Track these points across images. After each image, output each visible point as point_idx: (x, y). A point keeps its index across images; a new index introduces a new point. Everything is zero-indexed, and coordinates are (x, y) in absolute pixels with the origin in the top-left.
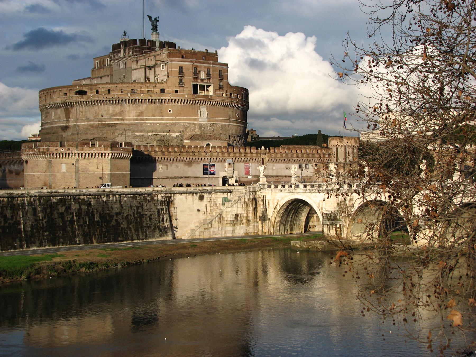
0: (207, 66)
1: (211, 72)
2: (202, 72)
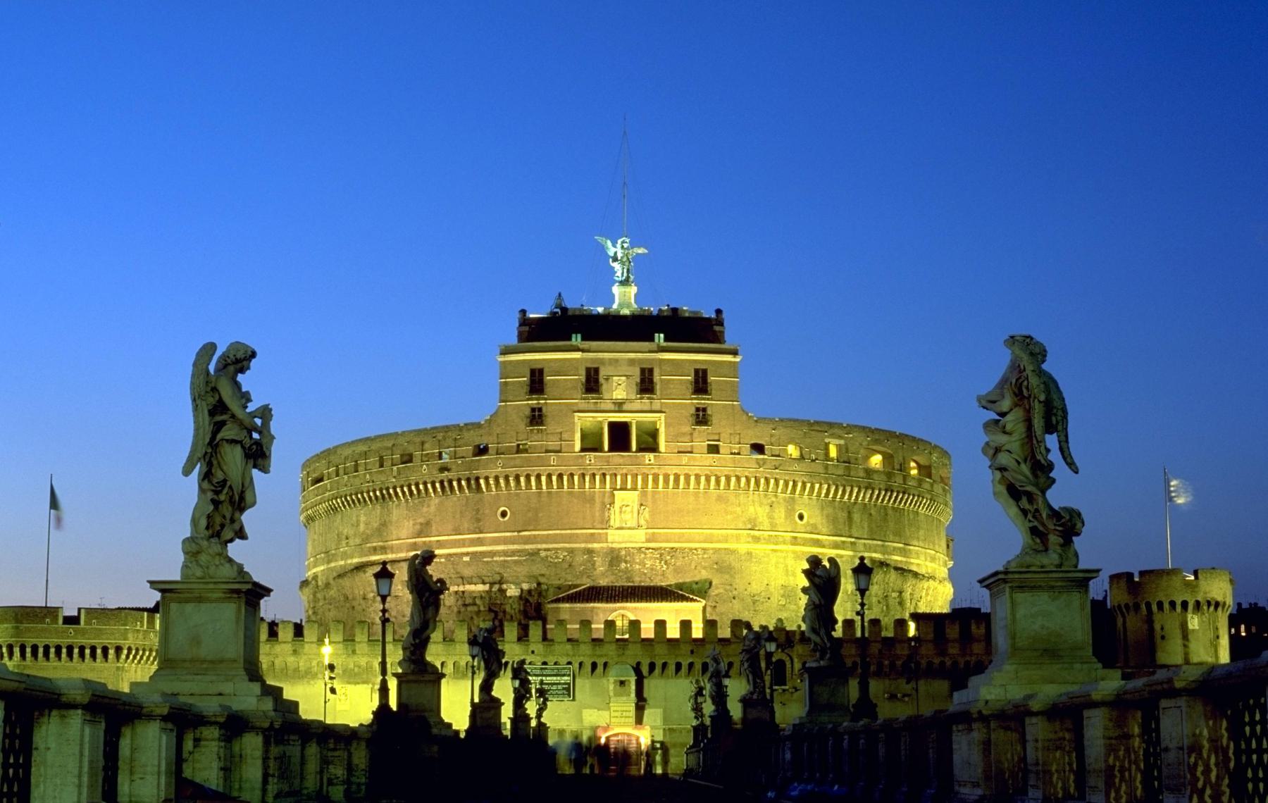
0: (640, 361)
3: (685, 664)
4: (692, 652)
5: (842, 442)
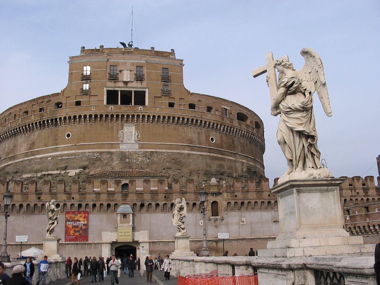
1: (145, 71)
2: (125, 72)
3: (161, 204)
4: (165, 197)
5: (229, 108)
